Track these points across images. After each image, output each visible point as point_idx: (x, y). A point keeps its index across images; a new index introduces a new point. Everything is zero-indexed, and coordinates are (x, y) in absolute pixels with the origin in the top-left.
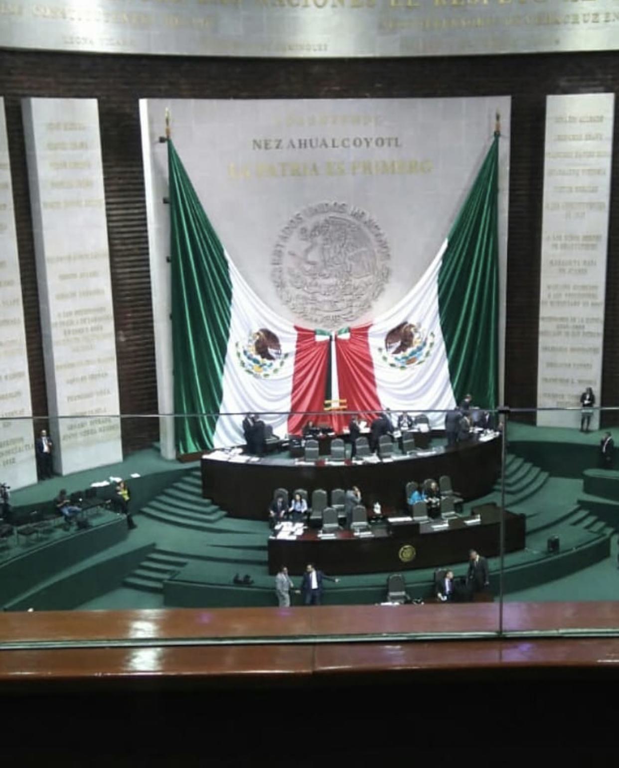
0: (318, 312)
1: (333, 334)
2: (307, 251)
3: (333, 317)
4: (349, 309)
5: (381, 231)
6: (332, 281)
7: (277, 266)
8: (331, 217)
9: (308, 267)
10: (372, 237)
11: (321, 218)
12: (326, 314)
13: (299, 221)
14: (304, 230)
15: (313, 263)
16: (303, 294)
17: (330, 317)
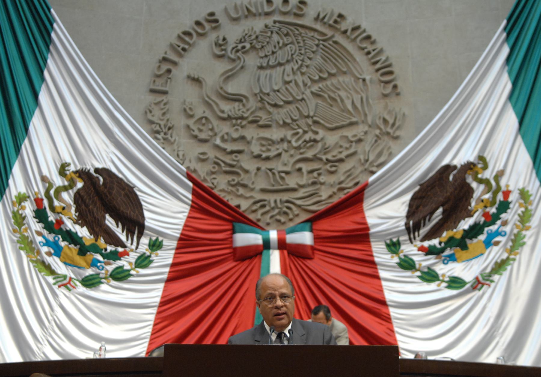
0: (241, 191)
1: (273, 235)
2: (228, 77)
3: (275, 202)
4: (311, 189)
5: (379, 46)
6: (275, 134)
7: (159, 98)
8: (275, 22)
9: (227, 107)
10: (359, 57)
11: (258, 24)
12: (259, 196)
13: (214, 25)
14: (221, 44)
15: (237, 99)
16: (212, 154)
17: (269, 202)
